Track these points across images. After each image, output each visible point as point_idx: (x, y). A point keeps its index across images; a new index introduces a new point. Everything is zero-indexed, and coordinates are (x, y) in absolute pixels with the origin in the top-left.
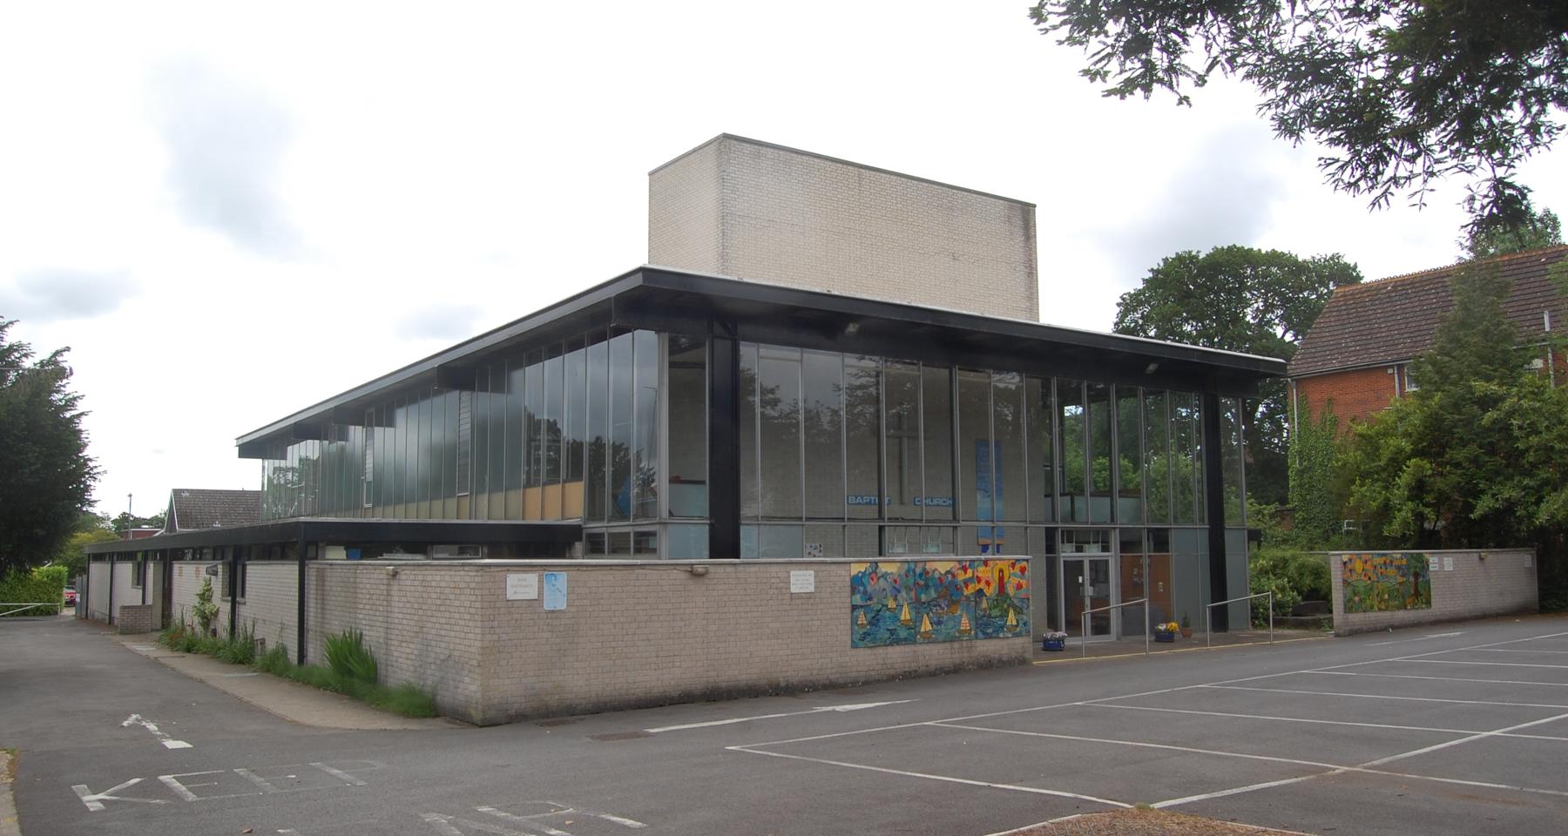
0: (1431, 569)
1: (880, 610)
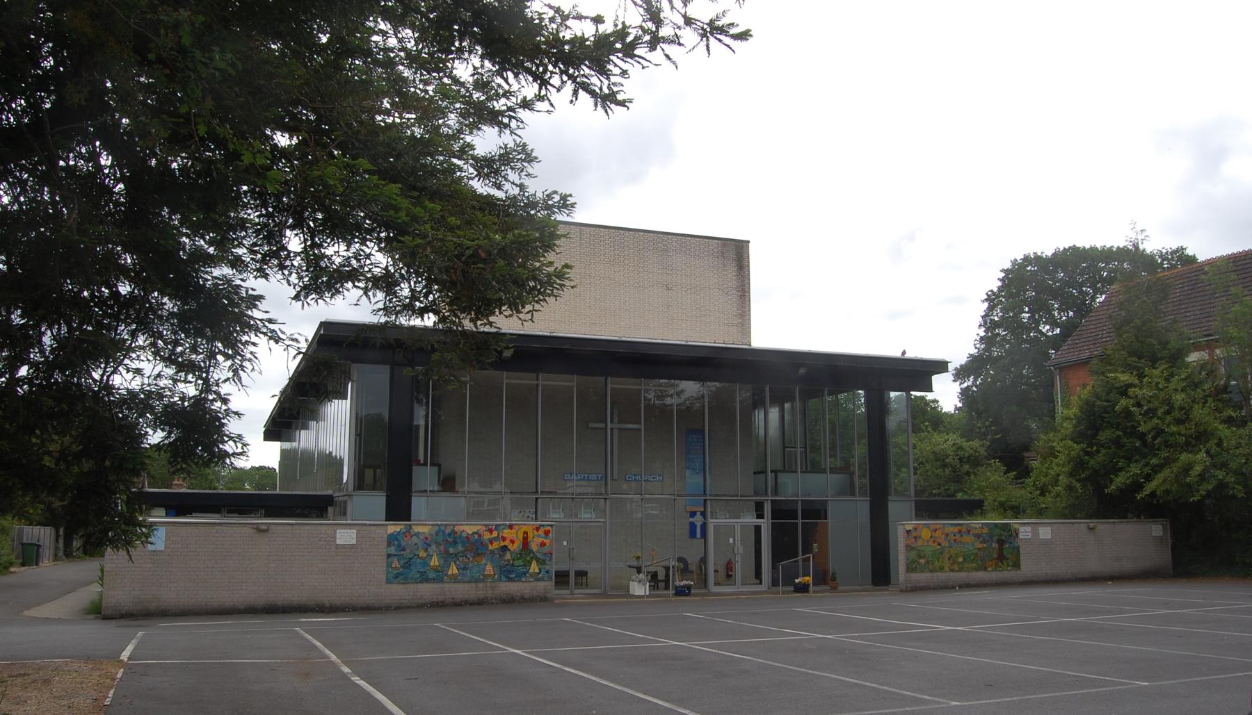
0: (1021, 537)
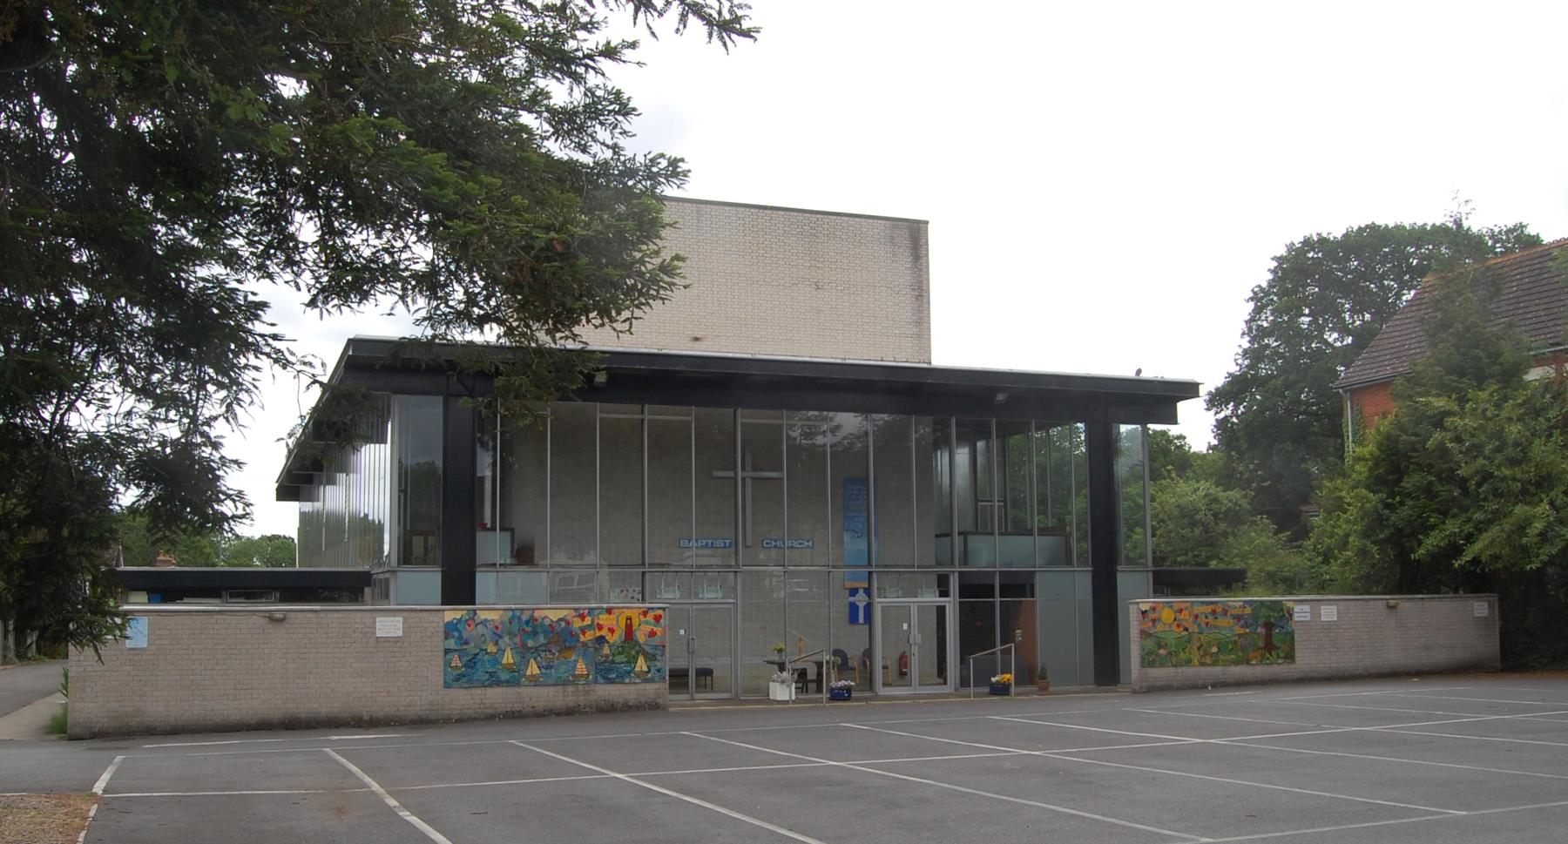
1: (477, 654)
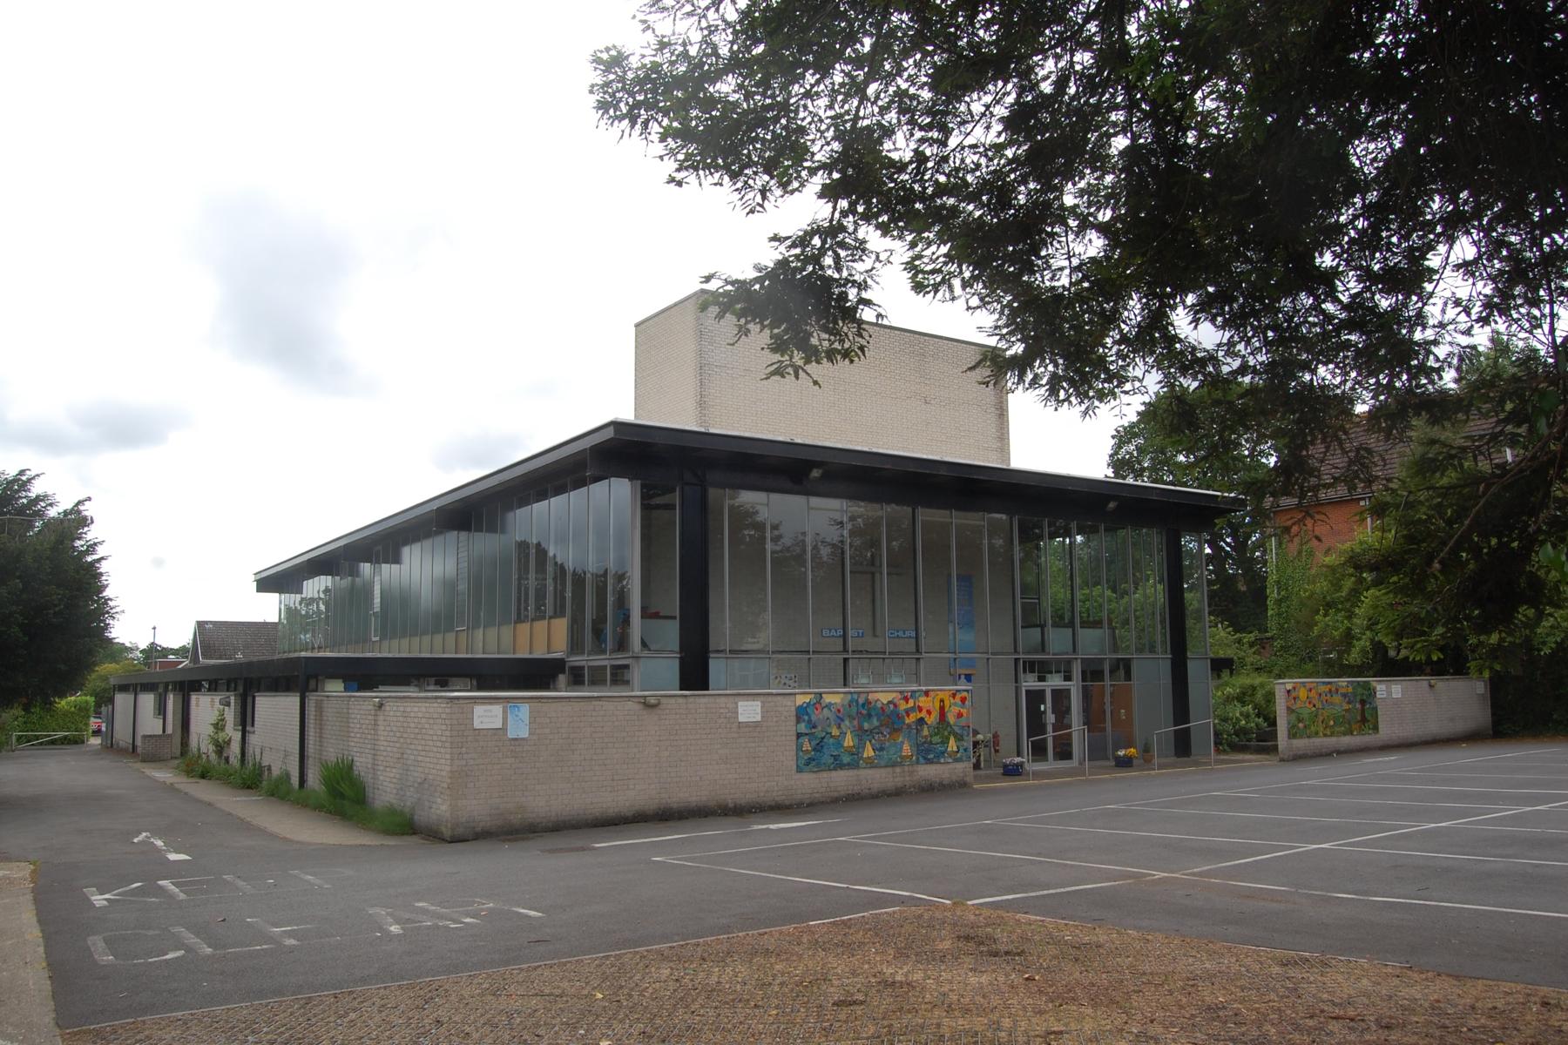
0: (1378, 696)
1: (823, 738)
